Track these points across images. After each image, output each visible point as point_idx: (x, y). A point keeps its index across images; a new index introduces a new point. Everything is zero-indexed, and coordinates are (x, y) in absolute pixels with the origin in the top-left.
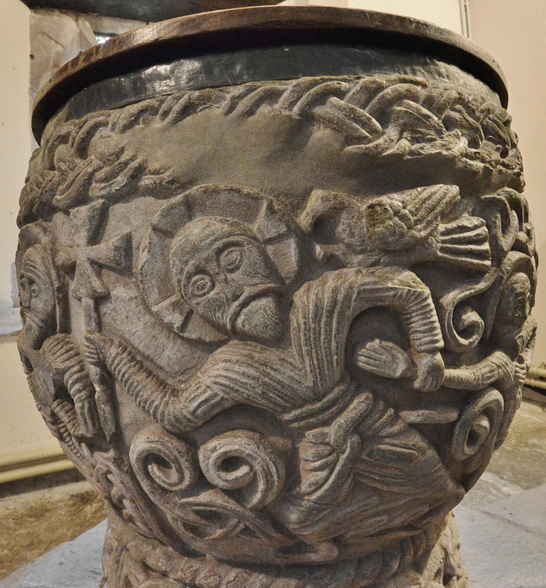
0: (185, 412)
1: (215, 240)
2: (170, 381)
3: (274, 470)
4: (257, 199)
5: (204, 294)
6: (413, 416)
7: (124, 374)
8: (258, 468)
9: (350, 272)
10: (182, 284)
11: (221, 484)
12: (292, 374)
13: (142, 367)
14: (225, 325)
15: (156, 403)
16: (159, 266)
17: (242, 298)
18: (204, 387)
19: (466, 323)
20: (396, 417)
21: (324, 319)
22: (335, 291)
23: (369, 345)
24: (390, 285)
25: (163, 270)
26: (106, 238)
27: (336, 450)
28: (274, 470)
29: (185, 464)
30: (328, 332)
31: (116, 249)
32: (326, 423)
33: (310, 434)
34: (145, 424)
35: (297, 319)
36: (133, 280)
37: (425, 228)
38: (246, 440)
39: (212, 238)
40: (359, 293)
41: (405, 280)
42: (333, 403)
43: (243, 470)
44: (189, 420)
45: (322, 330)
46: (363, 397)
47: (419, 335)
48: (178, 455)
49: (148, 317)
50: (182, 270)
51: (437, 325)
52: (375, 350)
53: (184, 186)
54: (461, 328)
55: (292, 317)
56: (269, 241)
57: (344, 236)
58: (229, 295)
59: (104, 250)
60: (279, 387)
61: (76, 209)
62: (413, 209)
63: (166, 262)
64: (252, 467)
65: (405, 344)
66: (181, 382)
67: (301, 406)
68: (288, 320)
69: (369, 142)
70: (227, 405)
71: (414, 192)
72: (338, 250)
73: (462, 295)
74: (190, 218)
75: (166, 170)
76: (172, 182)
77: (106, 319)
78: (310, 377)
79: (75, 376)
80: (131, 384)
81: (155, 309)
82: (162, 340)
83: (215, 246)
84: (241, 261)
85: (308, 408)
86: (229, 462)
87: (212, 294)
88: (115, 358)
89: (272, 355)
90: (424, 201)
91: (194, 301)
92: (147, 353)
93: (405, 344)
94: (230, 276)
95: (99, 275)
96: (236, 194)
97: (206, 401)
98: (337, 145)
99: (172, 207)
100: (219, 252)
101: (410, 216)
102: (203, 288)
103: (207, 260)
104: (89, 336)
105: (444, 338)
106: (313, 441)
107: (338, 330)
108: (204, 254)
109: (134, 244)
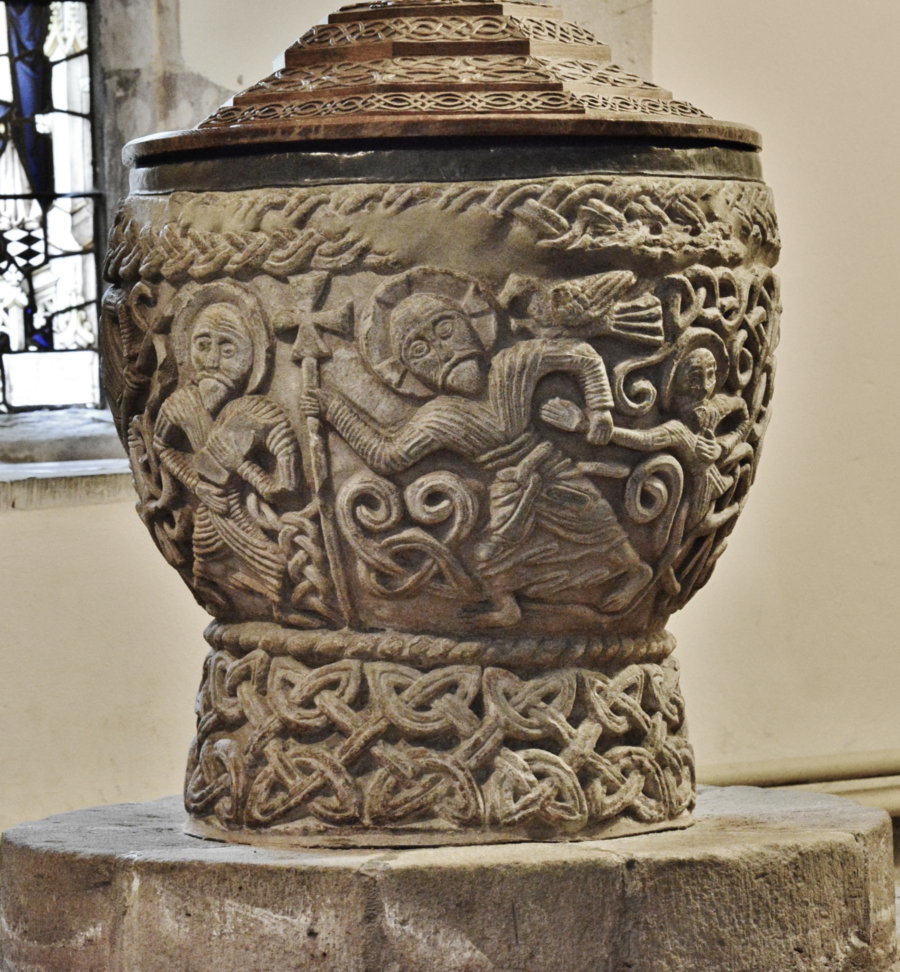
0: (400, 453)
1: (433, 313)
2: (381, 431)
3: (470, 503)
4: (466, 281)
5: (422, 356)
6: (587, 467)
7: (347, 422)
8: (457, 501)
9: (537, 342)
10: (403, 347)
11: (424, 517)
12: (489, 421)
13: (359, 418)
14: (436, 381)
15: (374, 446)
16: (380, 332)
17: (453, 360)
18: (417, 431)
19: (636, 390)
20: (573, 466)
21: (515, 379)
22: (525, 357)
23: (550, 401)
24: (568, 354)
25: (384, 335)
26: (327, 305)
27: (521, 486)
28: (470, 503)
29: (393, 499)
30: (518, 389)
31: (344, 316)
32: (514, 464)
33: (500, 474)
34: (356, 469)
35: (494, 378)
36: (354, 343)
37: (599, 308)
38: (449, 477)
39: (431, 312)
40: (543, 359)
41: (583, 350)
42: (520, 446)
43: (445, 503)
44: (402, 459)
45: (514, 388)
46: (544, 444)
47: (592, 396)
48: (388, 492)
49: (366, 375)
50: (404, 336)
51: (607, 387)
52: (555, 406)
53: (404, 268)
54: (632, 393)
55: (490, 376)
56: (474, 315)
57: (534, 313)
58: (442, 358)
59: (331, 315)
60: (479, 431)
61: (300, 277)
62: (590, 294)
63: (387, 330)
64: (451, 501)
65: (582, 403)
66: (392, 432)
67: (495, 448)
68: (487, 380)
69: (557, 237)
70: (436, 446)
71: (591, 278)
72: (529, 324)
73: (633, 365)
74: (410, 293)
75: (390, 252)
76: (396, 263)
77: (327, 377)
78: (503, 424)
79: (284, 431)
80: (353, 430)
81: (376, 367)
82: (378, 395)
83: (432, 319)
84: (452, 331)
85: (501, 449)
86: (433, 496)
87: (428, 356)
88: (338, 409)
89: (474, 406)
90: (599, 287)
91: (412, 362)
92: (363, 406)
93: (582, 403)
94: (444, 343)
95: (321, 337)
96: (450, 277)
97: (419, 442)
98: (531, 240)
99: (396, 285)
100: (435, 323)
101: (587, 300)
102: (420, 351)
103: (426, 329)
104: (311, 390)
105: (614, 400)
106: (503, 478)
107: (526, 386)
108: (425, 324)
109: (356, 311)
